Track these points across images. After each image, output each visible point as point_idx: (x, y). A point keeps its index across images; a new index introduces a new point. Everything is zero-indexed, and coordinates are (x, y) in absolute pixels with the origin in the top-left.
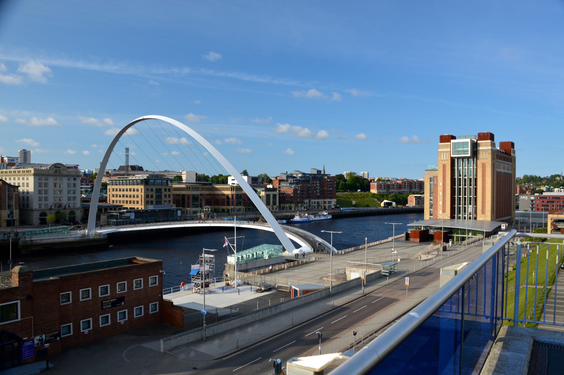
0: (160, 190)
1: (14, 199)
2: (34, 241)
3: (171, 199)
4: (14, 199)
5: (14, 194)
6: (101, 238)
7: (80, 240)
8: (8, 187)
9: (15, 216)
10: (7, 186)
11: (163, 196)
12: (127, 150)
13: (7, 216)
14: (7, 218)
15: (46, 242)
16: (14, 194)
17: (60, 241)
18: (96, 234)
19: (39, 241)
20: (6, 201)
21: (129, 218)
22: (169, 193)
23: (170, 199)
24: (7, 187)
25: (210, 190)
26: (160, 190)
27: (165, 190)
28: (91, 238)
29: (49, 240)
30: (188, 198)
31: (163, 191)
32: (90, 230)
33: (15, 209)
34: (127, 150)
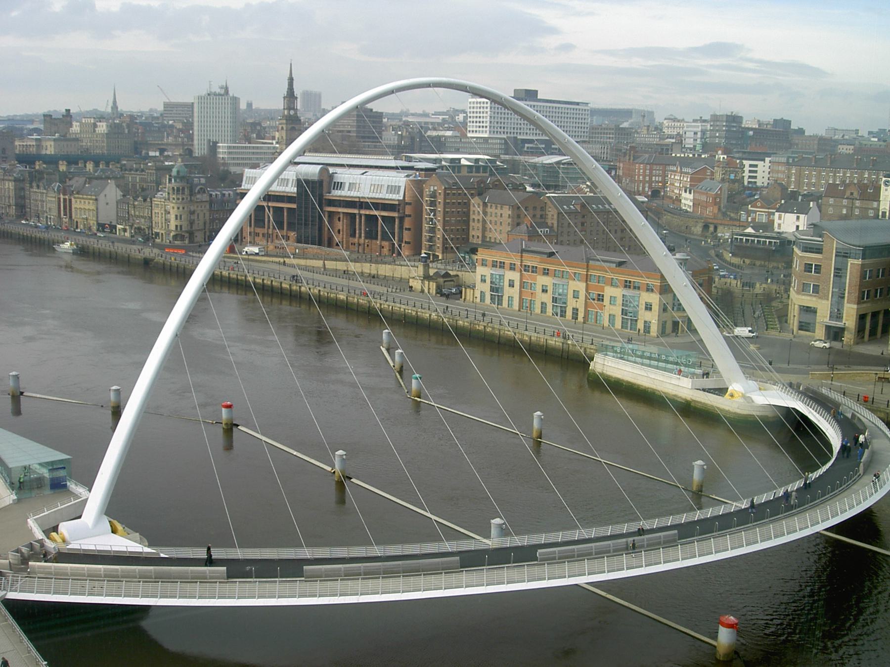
4: (848, 277)
5: (849, 264)
13: (828, 316)
14: (827, 320)
33: (847, 303)
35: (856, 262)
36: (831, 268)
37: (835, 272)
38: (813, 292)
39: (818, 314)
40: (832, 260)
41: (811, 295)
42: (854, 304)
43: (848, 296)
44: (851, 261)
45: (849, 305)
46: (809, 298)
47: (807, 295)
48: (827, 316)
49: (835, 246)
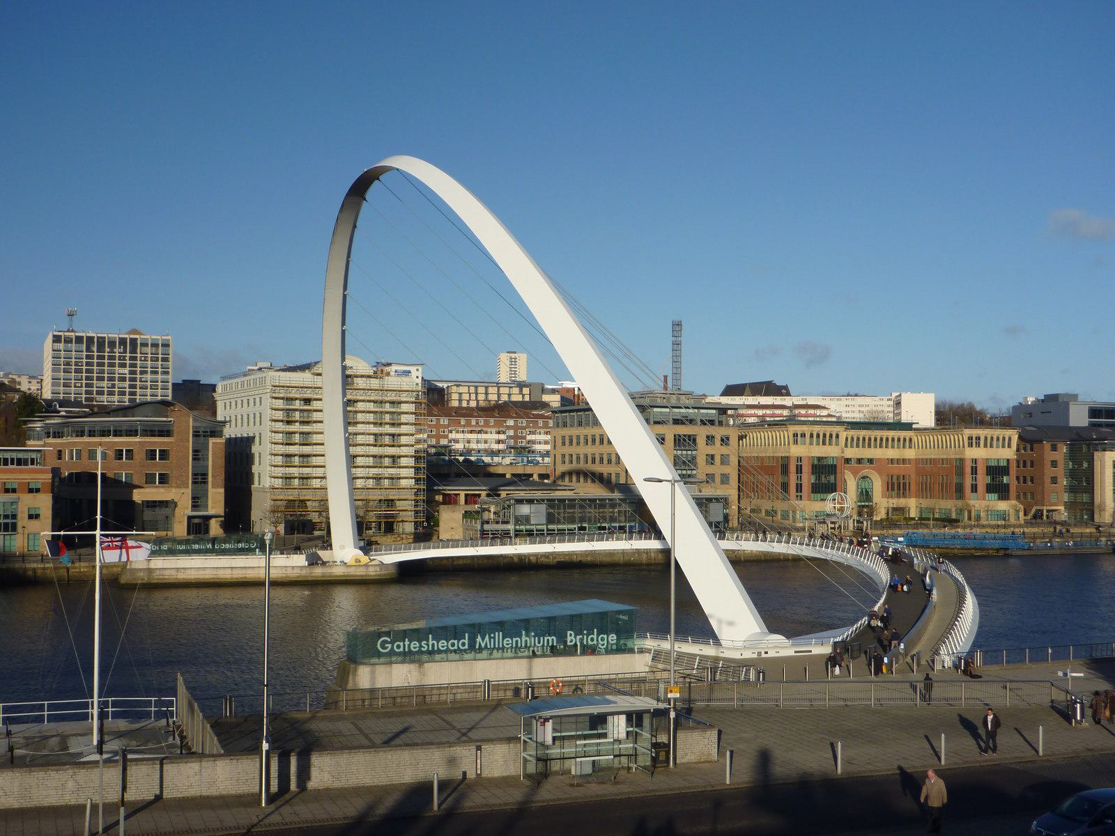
0: (692, 439)
2: (158, 572)
3: (732, 470)
5: (211, 444)
6: (371, 573)
7: (298, 577)
10: (191, 420)
11: (701, 460)
12: (677, 326)
14: (189, 512)
15: (192, 577)
17: (235, 576)
19: (173, 572)
21: (527, 519)
22: (725, 450)
23: (726, 470)
25: (863, 447)
26: (692, 439)
27: (710, 439)
28: (337, 574)
29: (201, 572)
30: (799, 469)
31: (701, 441)
33: (213, 487)
34: (677, 326)
36: (188, 450)
37: (193, 455)
40: (188, 442)
41: (157, 487)
42: (221, 488)
44: (212, 441)
45: (214, 490)
46: (154, 490)
48: (188, 507)
49: (191, 425)
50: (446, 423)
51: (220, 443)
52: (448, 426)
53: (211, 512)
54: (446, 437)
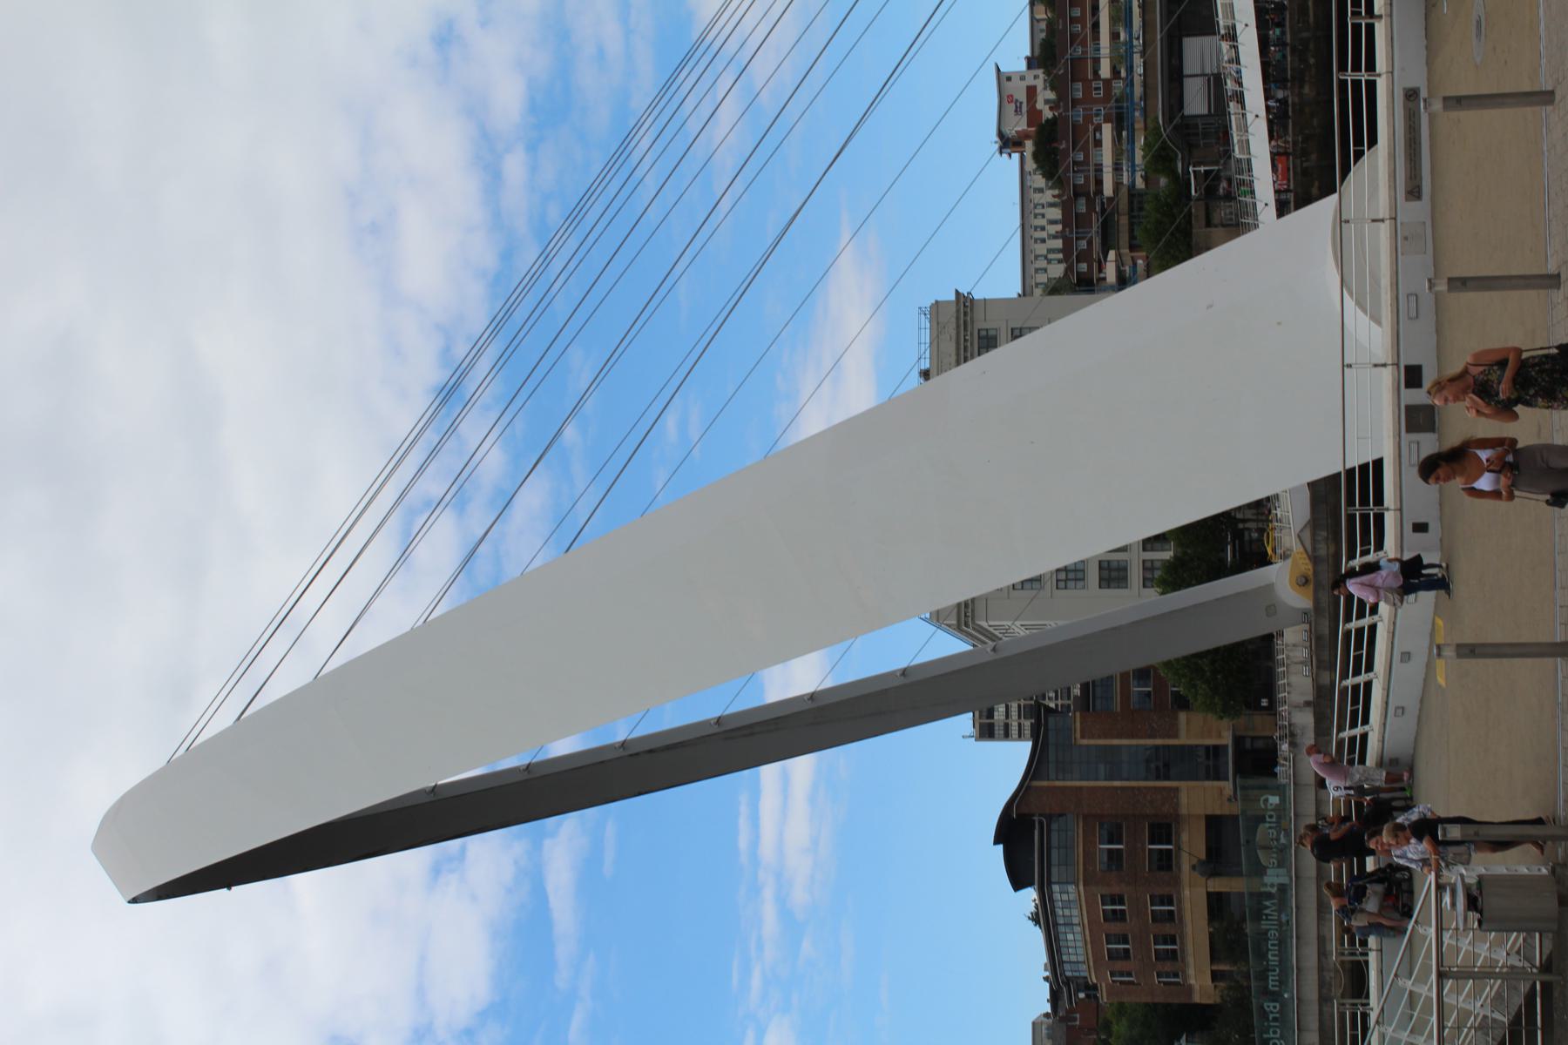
1: (1116, 742)
4: (1116, 742)
5: (1085, 742)
8: (1036, 780)
9: (1219, 736)
10: (1036, 783)
13: (1216, 783)
14: (1227, 786)
16: (1085, 742)
18: (1307, 581)
20: (1123, 788)
24: (1045, 783)
32: (1271, 609)
33: (1176, 736)
35: (1078, 724)
38: (1169, 842)
39: (1218, 812)
40: (1081, 788)
41: (1179, 848)
42: (1176, 718)
43: (1162, 737)
47: (1179, 857)
50: (1079, 85)
51: (1081, 723)
52: (1085, 81)
53: (1227, 739)
54: (1107, 82)
